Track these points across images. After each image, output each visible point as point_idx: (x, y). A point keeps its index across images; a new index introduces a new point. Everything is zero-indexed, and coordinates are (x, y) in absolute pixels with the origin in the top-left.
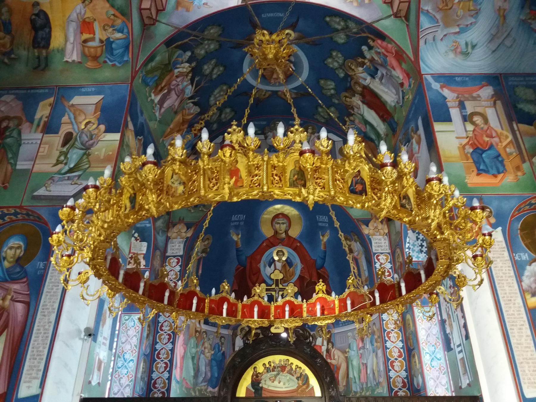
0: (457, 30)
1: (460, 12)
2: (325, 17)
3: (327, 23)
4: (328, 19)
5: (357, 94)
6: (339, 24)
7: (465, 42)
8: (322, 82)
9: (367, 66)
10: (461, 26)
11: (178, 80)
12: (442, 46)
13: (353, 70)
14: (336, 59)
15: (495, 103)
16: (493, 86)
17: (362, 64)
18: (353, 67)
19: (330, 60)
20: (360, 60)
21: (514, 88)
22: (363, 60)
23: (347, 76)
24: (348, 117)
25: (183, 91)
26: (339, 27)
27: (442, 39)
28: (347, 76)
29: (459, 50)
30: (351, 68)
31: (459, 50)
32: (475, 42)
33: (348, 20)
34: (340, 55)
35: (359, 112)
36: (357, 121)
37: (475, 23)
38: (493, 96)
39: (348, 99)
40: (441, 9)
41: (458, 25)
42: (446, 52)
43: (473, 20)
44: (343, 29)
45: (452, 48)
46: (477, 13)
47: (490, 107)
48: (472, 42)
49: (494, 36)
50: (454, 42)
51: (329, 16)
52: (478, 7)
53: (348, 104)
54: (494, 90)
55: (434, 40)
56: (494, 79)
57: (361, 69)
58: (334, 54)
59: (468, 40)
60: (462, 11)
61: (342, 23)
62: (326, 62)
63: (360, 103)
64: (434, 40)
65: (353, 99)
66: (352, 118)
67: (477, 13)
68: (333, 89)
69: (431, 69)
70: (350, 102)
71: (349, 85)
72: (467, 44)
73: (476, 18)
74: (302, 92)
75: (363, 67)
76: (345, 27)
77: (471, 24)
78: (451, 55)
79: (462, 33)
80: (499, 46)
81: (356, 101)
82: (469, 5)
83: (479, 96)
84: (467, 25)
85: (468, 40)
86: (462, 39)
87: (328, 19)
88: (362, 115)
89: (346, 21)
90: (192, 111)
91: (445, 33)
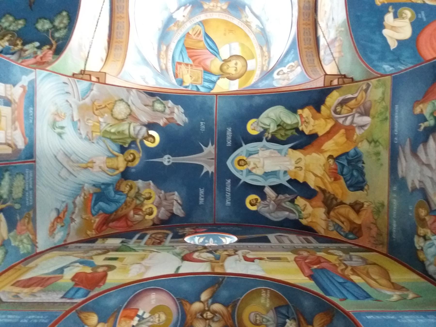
0: (76, 119)
1: (91, 123)
2: (66, 11)
3: (60, 13)
4: (64, 13)
6: (61, 22)
7: (64, 125)
10: (78, 123)
12: (61, 100)
15: (9, 145)
16: (24, 150)
21: (23, 174)
26: (56, 23)
27: (67, 101)
29: (58, 119)
31: (58, 119)
32: (64, 136)
34: (20, 27)
37: (81, 138)
38: (16, 146)
40: (93, 103)
41: (79, 120)
42: (56, 104)
43: (84, 136)
44: (54, 27)
45: (59, 112)
46: (90, 140)
47: (6, 139)
48: (63, 133)
49: (69, 158)
50: (65, 114)
51: (68, 15)
52: (95, 141)
54: (20, 150)
55: (67, 93)
56: (29, 155)
58: (21, 22)
59: (66, 130)
60: (92, 124)
62: (7, 15)
64: (67, 93)
67: (90, 140)
69: (42, 80)
72: (62, 128)
73: (86, 139)
77: (81, 134)
78: (53, 109)
79: (73, 124)
80: (61, 163)
82: (96, 132)
83: (16, 129)
84: (79, 130)
85: (66, 129)
86: (66, 123)
89: (65, 28)
91: (73, 105)
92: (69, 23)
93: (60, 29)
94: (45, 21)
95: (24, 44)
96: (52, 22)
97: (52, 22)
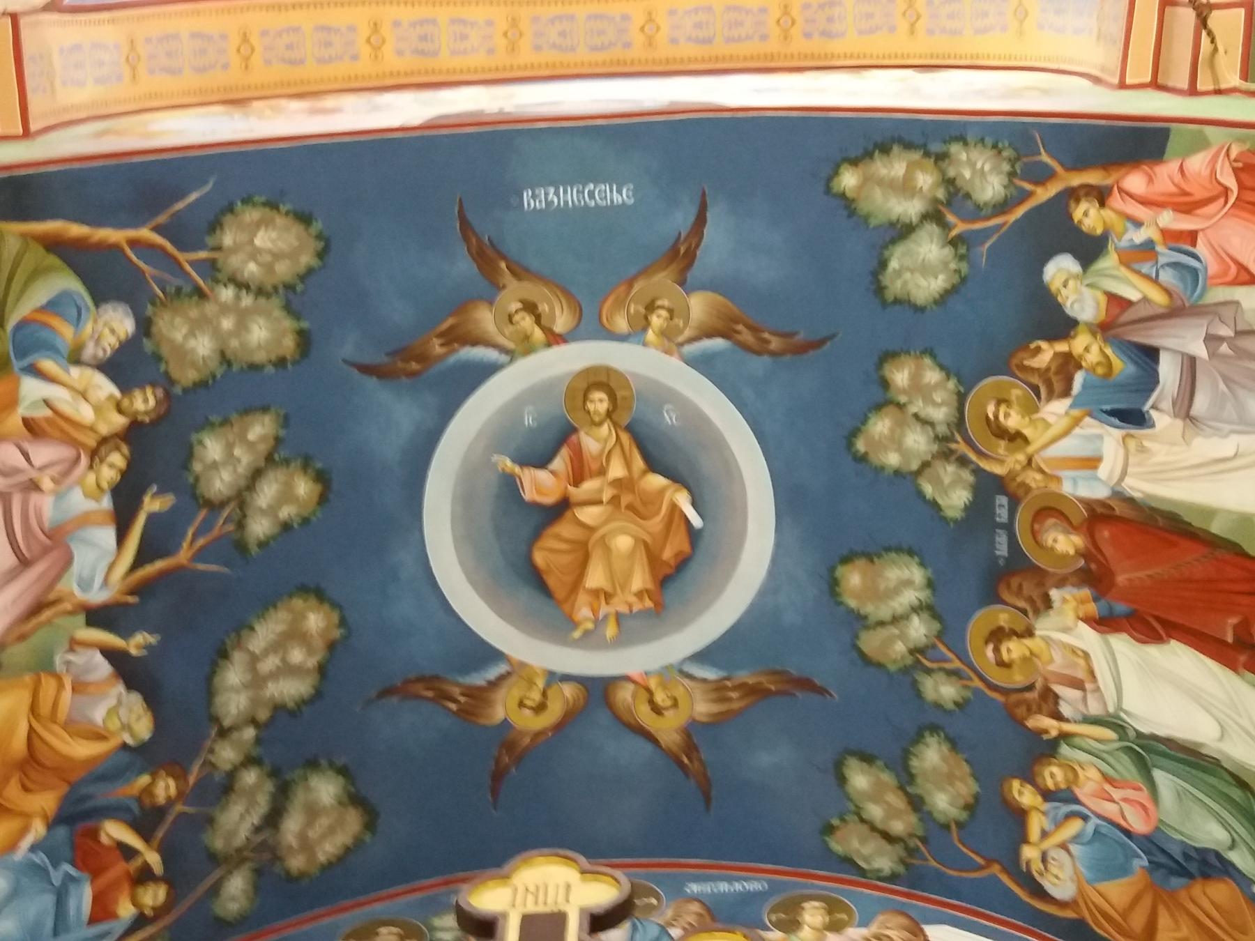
2: (836, 172)
3: (847, 204)
4: (849, 180)
5: (1061, 583)
6: (906, 188)
8: (853, 578)
9: (1092, 370)
11: (43, 453)
13: (1016, 438)
14: (917, 406)
17: (1060, 377)
18: (1013, 421)
19: (880, 426)
20: (1046, 354)
22: (1062, 347)
23: (988, 487)
24: (1029, 778)
25: (57, 542)
26: (911, 209)
28: (988, 487)
30: (1001, 433)
33: (955, 148)
34: (932, 376)
35: (1094, 709)
36: (1088, 784)
39: (1014, 649)
44: (934, 215)
51: (854, 162)
53: (1018, 678)
57: (1056, 410)
58: (900, 376)
61: (926, 180)
62: (861, 446)
63: (1087, 638)
65: (1045, 627)
66: (1053, 775)
68: (916, 609)
70: (1029, 659)
71: (1002, 549)
74: (745, 676)
75: (1066, 393)
76: (941, 194)
81: (1066, 631)
87: (849, 180)
88: (1114, 723)
90: (98, 714)
92: (908, 146)
93: (950, 183)
94: (894, 264)
95: (1063, 326)
96: (902, 231)
97: (902, 231)
